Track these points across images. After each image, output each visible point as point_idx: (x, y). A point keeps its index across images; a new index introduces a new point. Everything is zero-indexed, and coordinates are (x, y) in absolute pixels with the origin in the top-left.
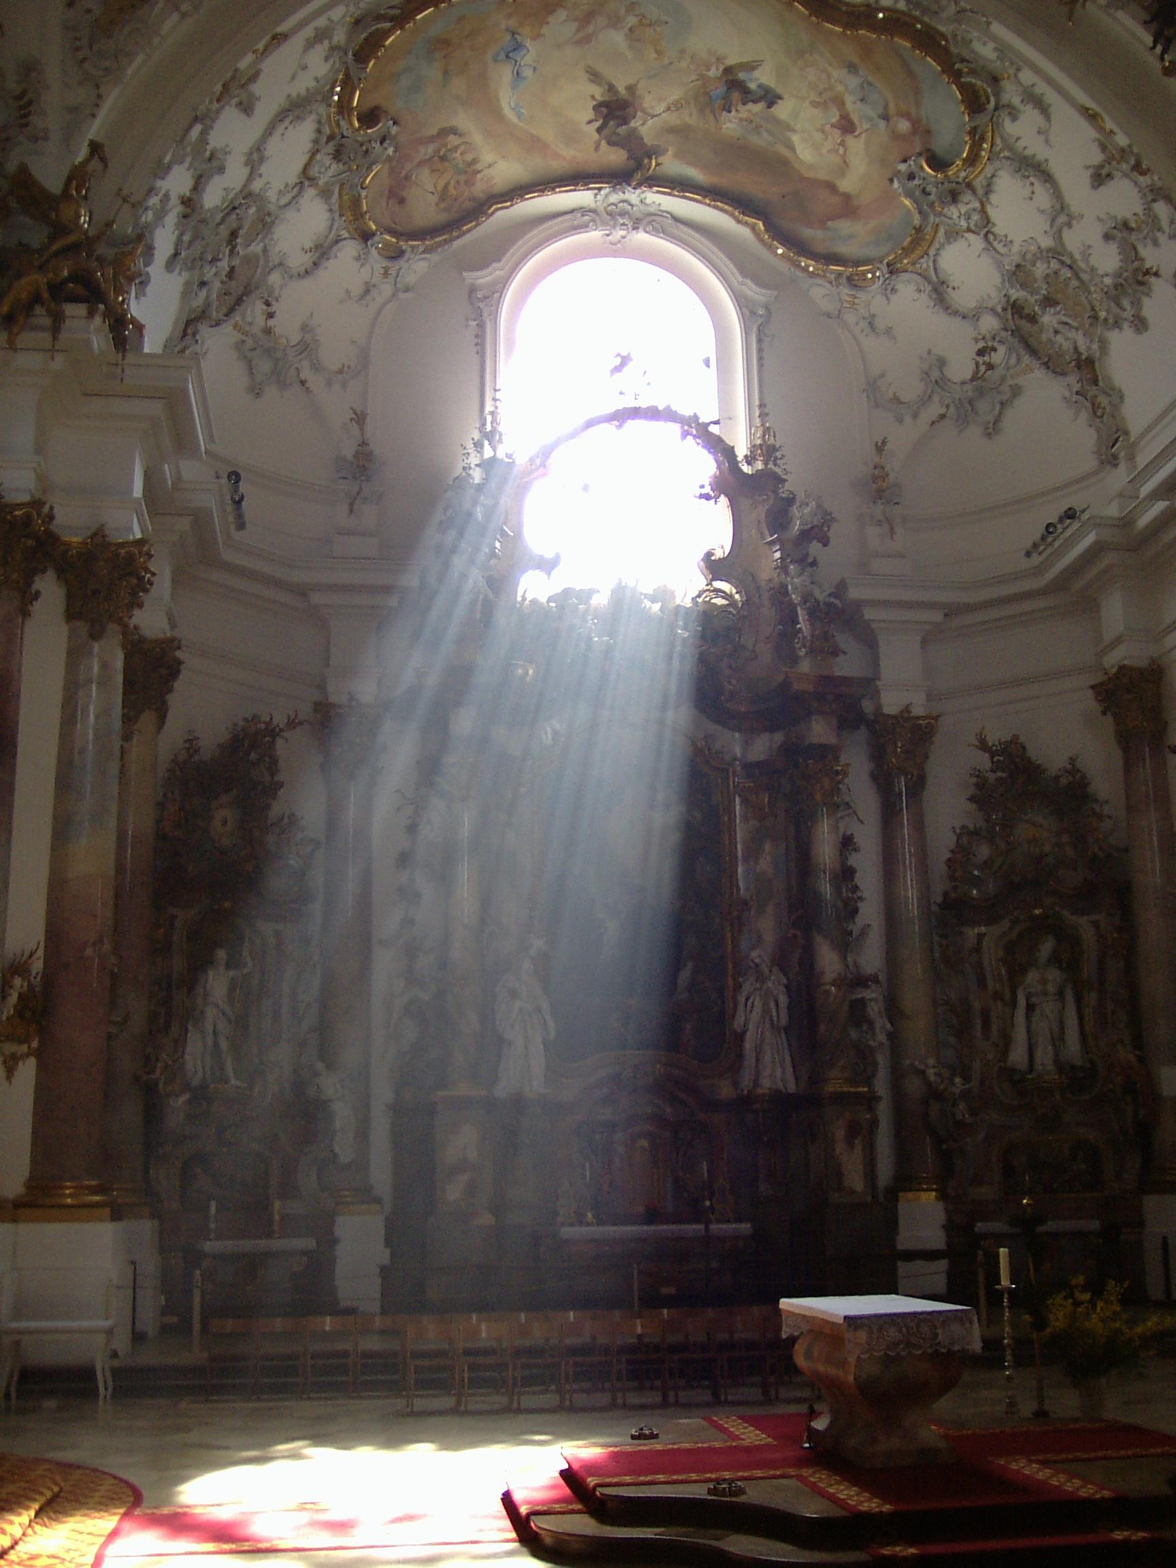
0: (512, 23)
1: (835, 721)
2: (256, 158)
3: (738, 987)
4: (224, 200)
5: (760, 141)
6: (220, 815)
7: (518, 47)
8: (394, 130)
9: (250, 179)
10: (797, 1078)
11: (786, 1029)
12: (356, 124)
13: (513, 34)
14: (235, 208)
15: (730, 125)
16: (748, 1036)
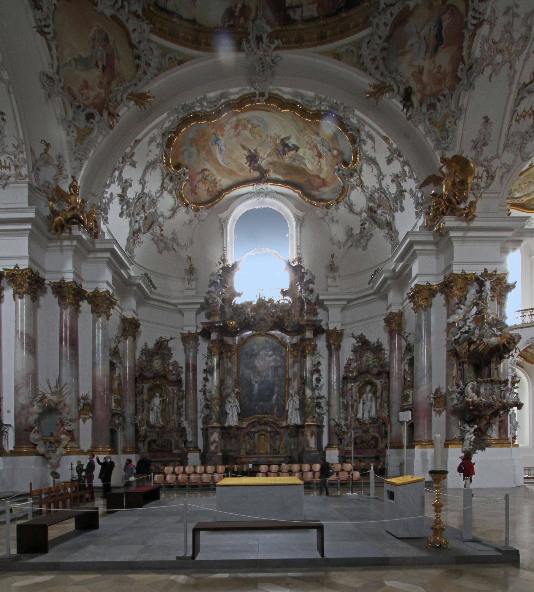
0: (214, 131)
1: (312, 332)
2: (143, 182)
3: (288, 399)
4: (136, 196)
5: (296, 164)
6: (156, 362)
7: (218, 139)
8: (187, 171)
9: (143, 189)
10: (301, 421)
11: (299, 409)
12: (173, 169)
13: (215, 135)
14: (140, 198)
15: (287, 159)
16: (289, 411)
